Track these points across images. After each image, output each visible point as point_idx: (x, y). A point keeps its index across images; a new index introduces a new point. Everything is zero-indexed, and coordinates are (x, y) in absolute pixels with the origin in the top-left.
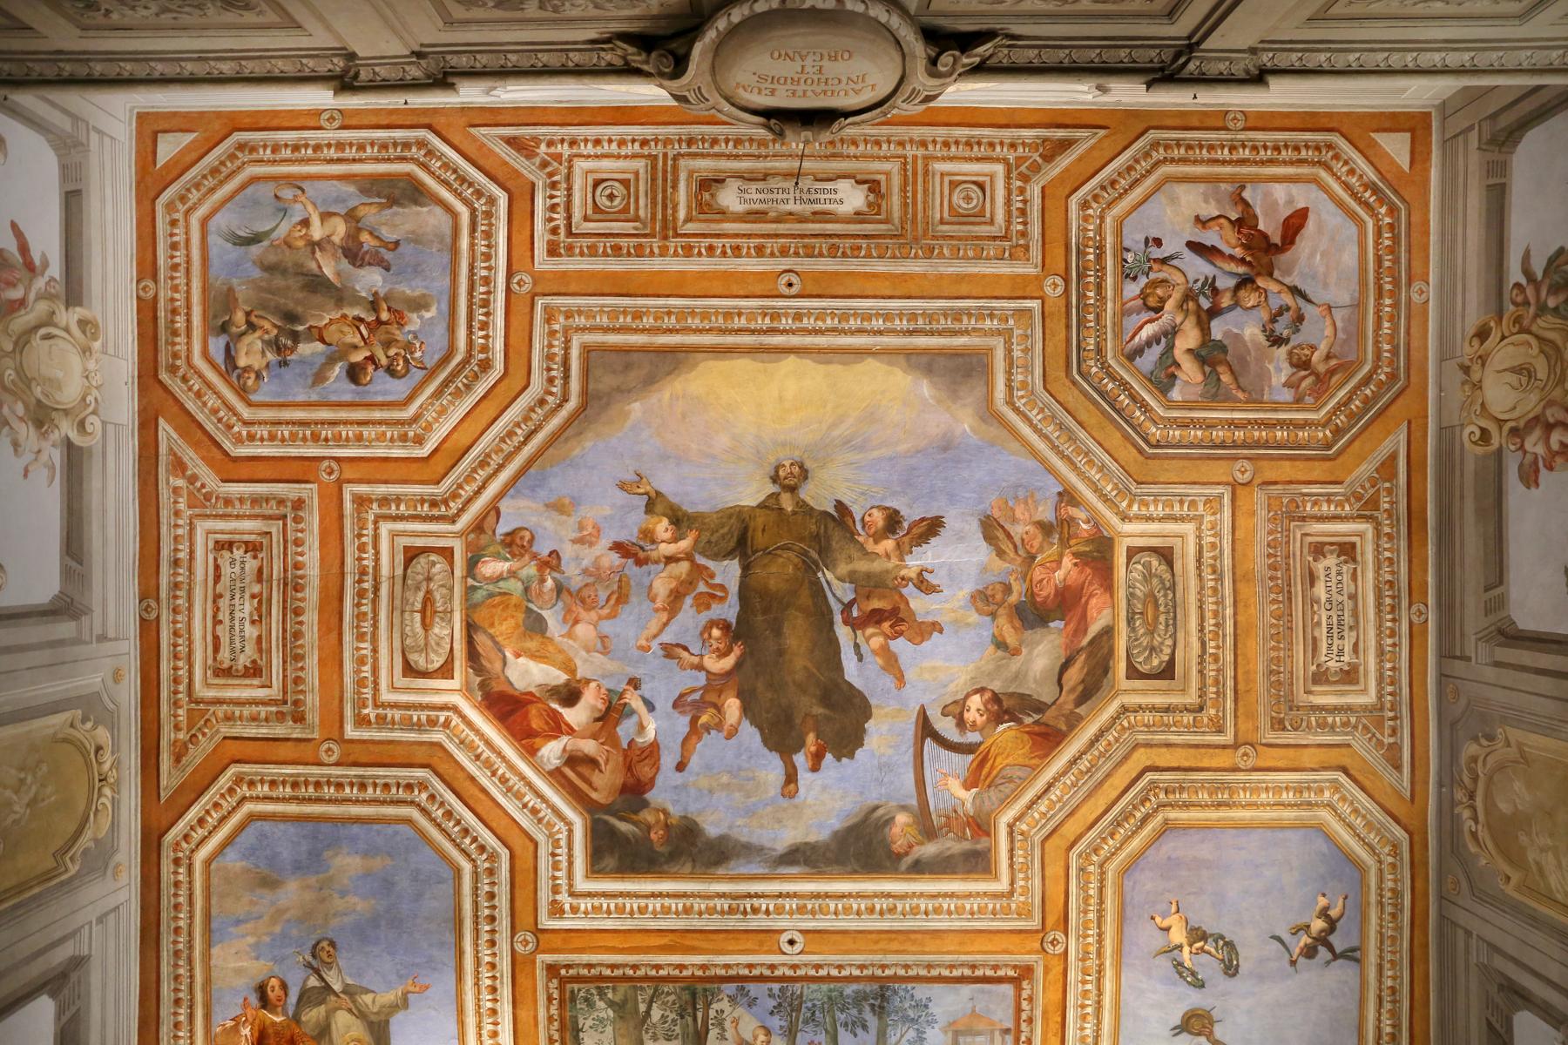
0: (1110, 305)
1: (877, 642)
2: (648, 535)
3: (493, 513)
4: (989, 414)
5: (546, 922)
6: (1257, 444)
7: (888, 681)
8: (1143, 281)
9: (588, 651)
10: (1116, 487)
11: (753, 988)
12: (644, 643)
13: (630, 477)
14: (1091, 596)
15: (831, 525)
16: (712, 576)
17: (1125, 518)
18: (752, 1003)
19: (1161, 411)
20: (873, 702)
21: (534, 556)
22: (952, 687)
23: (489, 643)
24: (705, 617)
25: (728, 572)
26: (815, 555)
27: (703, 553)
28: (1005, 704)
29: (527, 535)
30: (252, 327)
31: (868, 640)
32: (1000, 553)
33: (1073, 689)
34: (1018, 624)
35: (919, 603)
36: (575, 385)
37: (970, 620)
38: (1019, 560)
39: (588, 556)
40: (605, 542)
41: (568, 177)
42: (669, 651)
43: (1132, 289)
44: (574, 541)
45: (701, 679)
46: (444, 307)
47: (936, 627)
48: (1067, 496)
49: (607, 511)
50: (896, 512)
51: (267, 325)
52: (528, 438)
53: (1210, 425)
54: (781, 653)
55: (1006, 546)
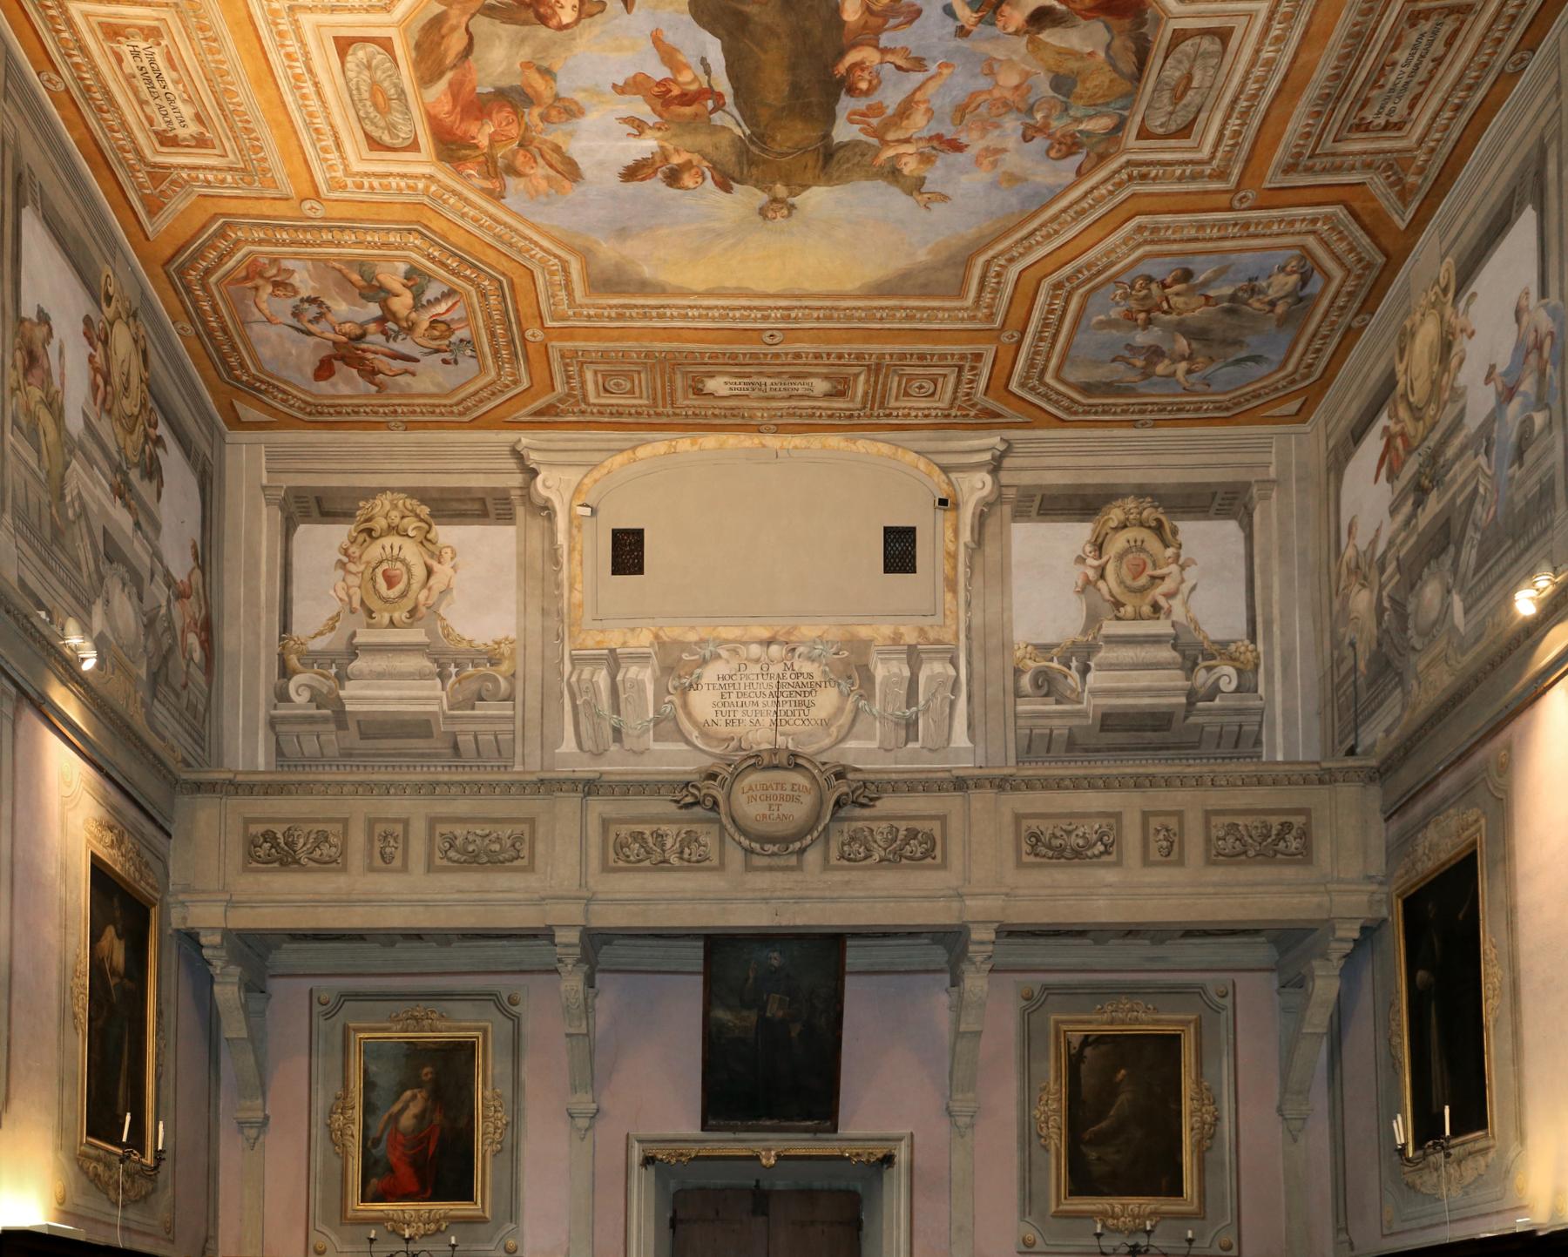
0: (481, 324)
1: (685, 77)
2: (926, 159)
3: (1083, 170)
4: (586, 255)
6: (305, 229)
7: (670, 38)
8: (453, 339)
9: (1010, 60)
10: (445, 202)
12: (946, 71)
13: (934, 206)
14: (450, 113)
15: (737, 175)
16: (861, 130)
17: (431, 178)
19: (414, 255)
20: (688, 17)
21: (1050, 136)
22: (596, 30)
23: (1121, 65)
24: (874, 99)
25: (844, 132)
26: (753, 148)
27: (869, 145)
28: (531, 14)
29: (1053, 154)
30: (1273, 304)
31: (696, 78)
32: (557, 149)
33: (453, 29)
34: (529, 91)
35: (641, 108)
36: (977, 272)
37: (582, 95)
38: (536, 143)
39: (992, 139)
40: (971, 152)
41: (955, 398)
42: (919, 64)
43: (463, 333)
44: (1004, 150)
45: (884, 40)
46: (1084, 323)
47: (620, 90)
48: (496, 196)
49: (964, 179)
50: (670, 185)
51: (1257, 305)
52: (1032, 233)
53: (359, 243)
54: (793, 68)
55: (555, 158)
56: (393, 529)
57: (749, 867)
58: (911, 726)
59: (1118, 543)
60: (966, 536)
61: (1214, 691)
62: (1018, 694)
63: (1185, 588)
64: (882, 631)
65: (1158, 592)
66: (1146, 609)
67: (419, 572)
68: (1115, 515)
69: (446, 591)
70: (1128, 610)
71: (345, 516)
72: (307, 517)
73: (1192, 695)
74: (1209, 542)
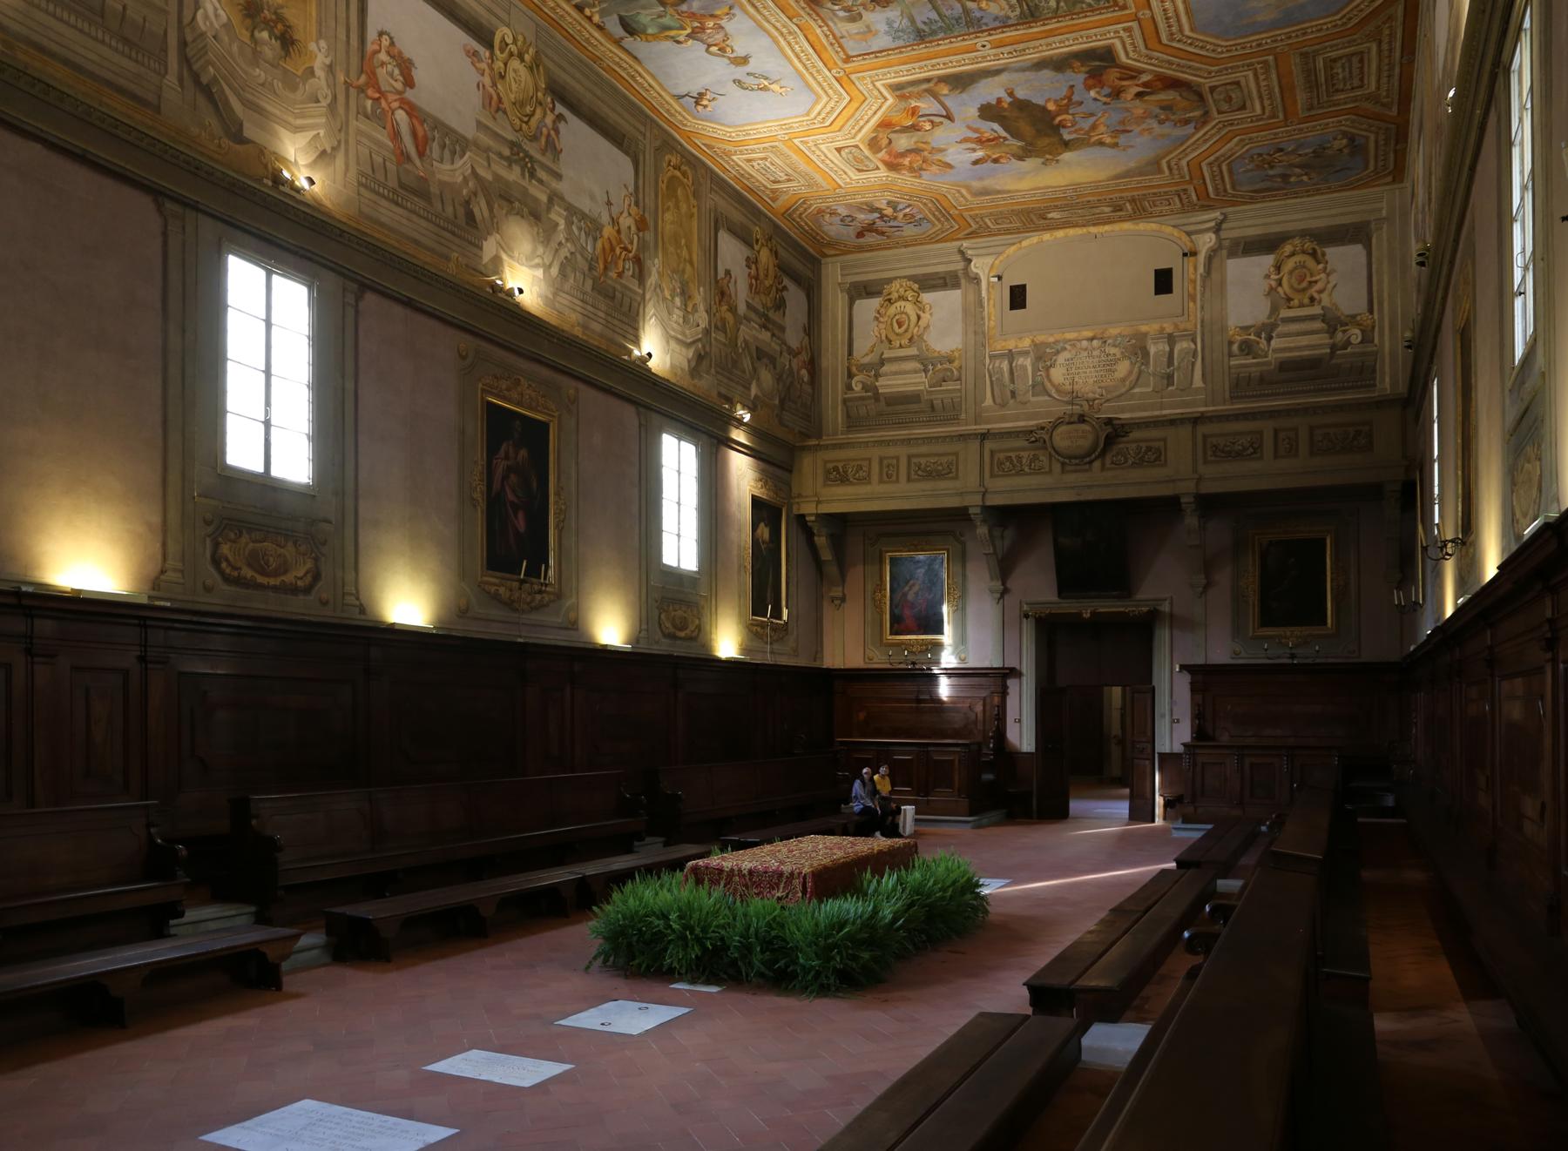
5: (1134, 24)
11: (997, 24)
18: (996, 18)
56: (902, 298)
57: (1063, 471)
58: (1169, 378)
59: (1290, 264)
60: (1201, 270)
61: (1348, 343)
62: (1231, 355)
63: (1330, 286)
64: (1150, 328)
65: (1313, 291)
66: (1306, 301)
67: (914, 318)
68: (1288, 249)
69: (927, 327)
70: (1296, 302)
71: (878, 293)
72: (860, 297)
73: (1333, 347)
74: (1345, 259)
